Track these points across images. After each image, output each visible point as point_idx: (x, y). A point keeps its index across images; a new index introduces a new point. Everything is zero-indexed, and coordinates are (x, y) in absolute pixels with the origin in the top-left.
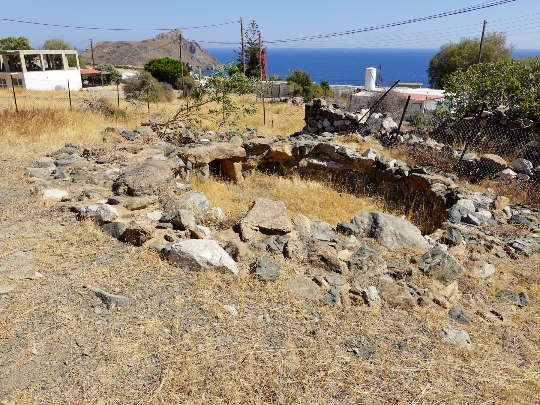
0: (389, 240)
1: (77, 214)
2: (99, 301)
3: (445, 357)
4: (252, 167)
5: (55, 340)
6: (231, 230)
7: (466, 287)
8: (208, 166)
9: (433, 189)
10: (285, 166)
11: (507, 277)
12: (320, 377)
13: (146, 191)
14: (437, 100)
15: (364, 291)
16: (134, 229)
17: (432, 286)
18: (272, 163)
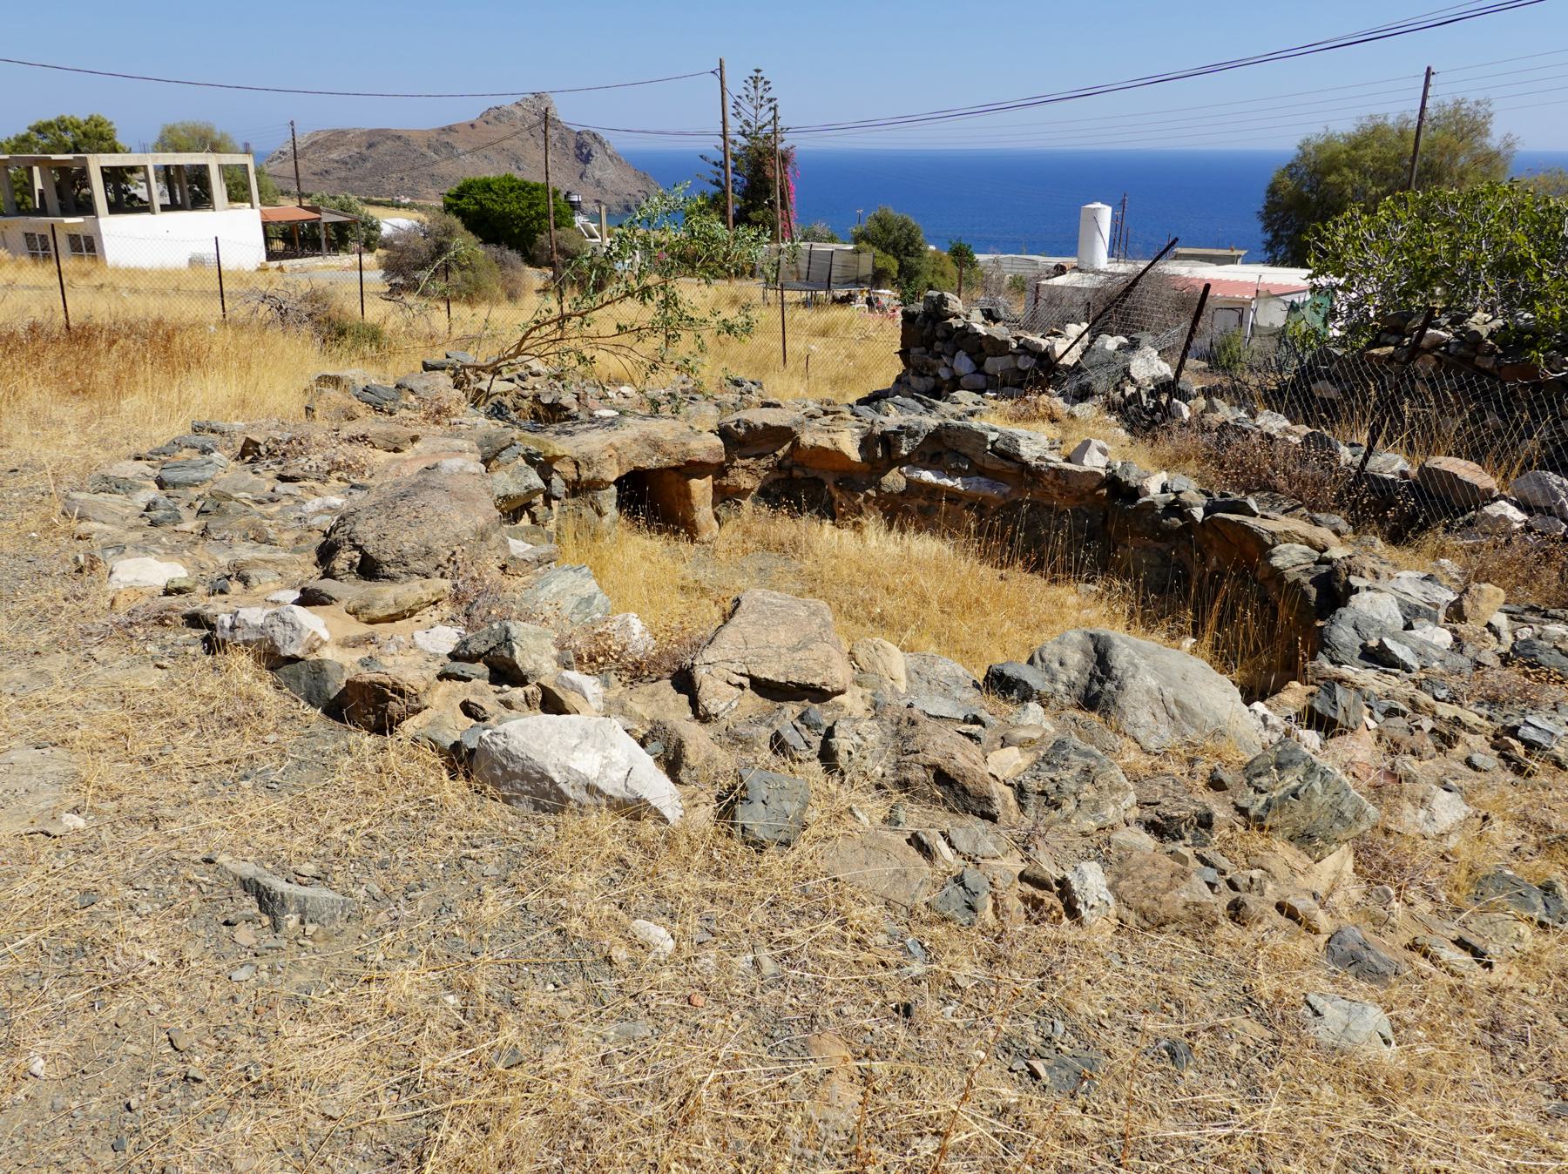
0: (1144, 717)
1: (206, 632)
2: (250, 905)
3: (1314, 1089)
4: (744, 493)
5: (106, 1028)
6: (666, 683)
7: (1377, 864)
8: (614, 489)
9: (1277, 562)
10: (841, 489)
11: (1503, 832)
12: (923, 1154)
13: (414, 565)
14: (1289, 299)
15: (1065, 879)
16: (371, 683)
17: (1273, 862)
18: (805, 483)
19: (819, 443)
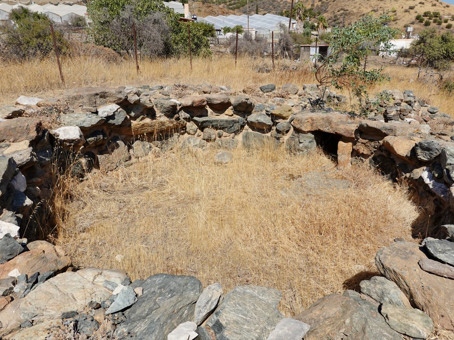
4: (366, 156)
19: (389, 141)
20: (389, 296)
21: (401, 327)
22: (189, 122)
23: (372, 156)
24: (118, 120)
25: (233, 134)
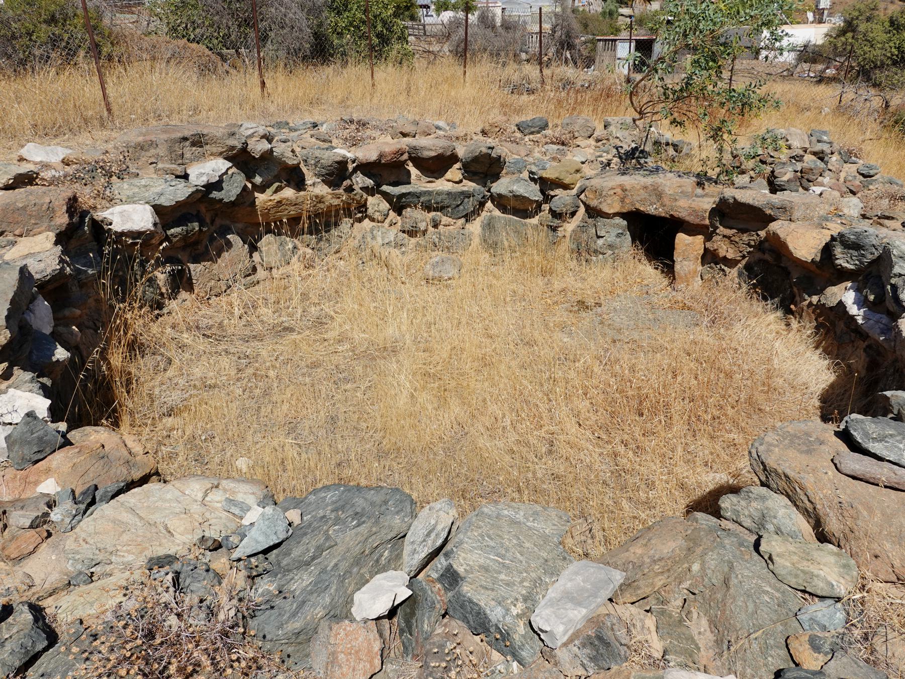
19: (778, 232)
20: (775, 521)
21: (796, 576)
22: (373, 195)
23: (744, 262)
24: (230, 191)
25: (463, 220)
